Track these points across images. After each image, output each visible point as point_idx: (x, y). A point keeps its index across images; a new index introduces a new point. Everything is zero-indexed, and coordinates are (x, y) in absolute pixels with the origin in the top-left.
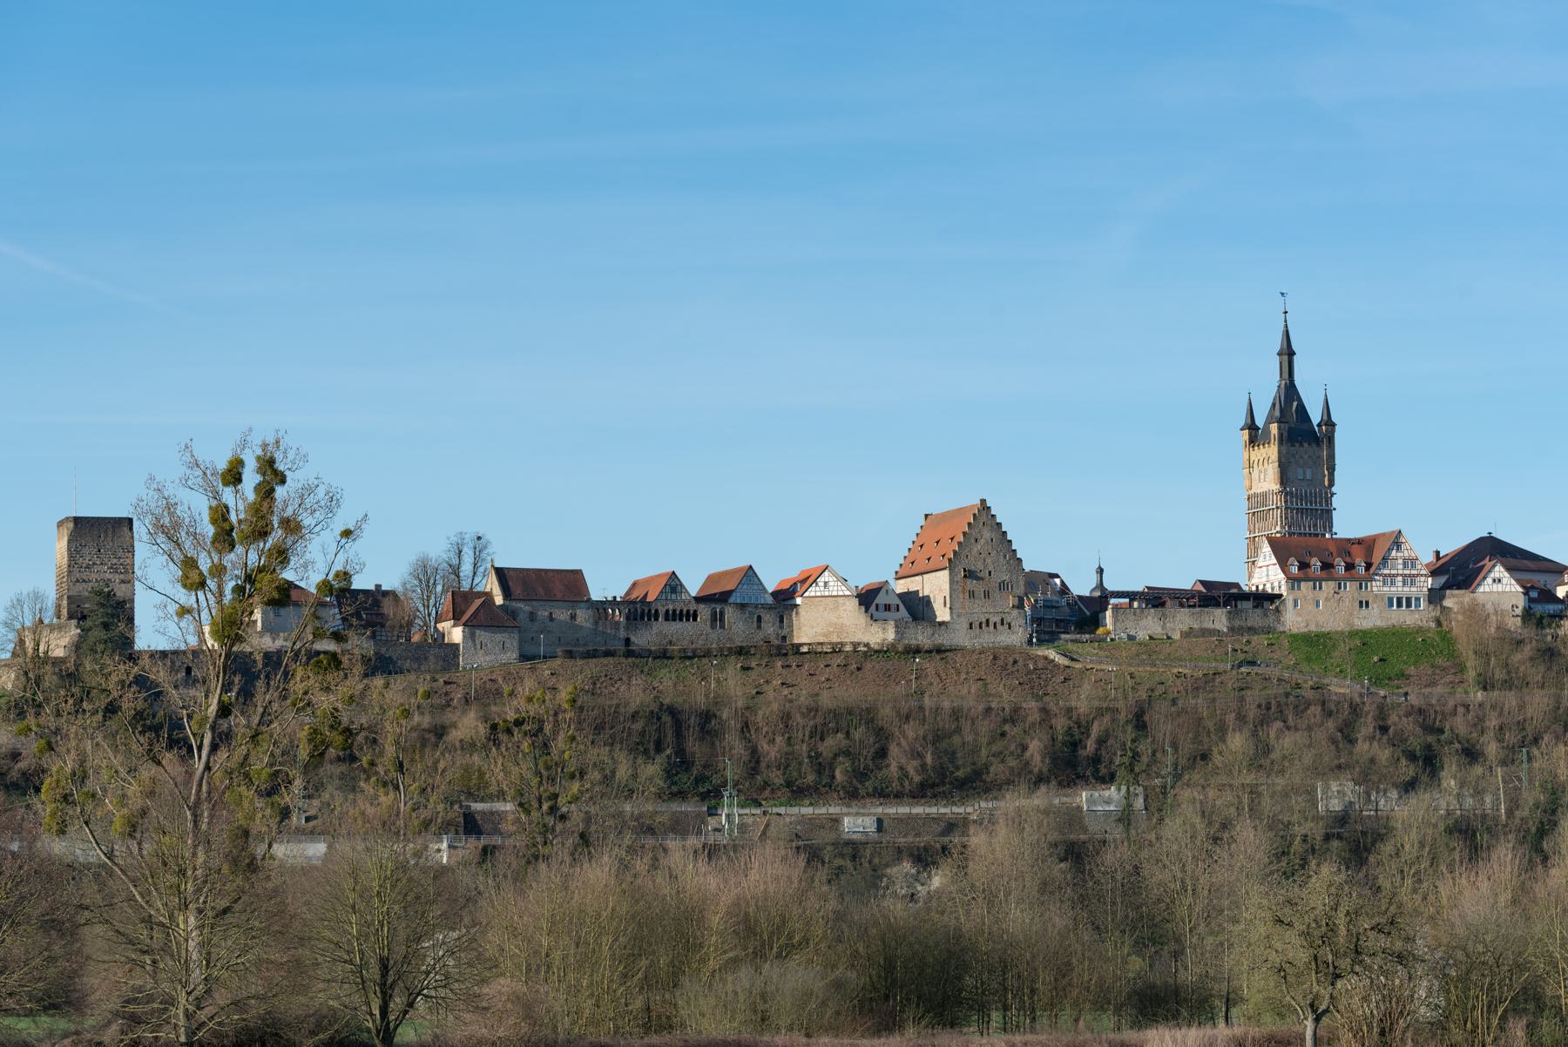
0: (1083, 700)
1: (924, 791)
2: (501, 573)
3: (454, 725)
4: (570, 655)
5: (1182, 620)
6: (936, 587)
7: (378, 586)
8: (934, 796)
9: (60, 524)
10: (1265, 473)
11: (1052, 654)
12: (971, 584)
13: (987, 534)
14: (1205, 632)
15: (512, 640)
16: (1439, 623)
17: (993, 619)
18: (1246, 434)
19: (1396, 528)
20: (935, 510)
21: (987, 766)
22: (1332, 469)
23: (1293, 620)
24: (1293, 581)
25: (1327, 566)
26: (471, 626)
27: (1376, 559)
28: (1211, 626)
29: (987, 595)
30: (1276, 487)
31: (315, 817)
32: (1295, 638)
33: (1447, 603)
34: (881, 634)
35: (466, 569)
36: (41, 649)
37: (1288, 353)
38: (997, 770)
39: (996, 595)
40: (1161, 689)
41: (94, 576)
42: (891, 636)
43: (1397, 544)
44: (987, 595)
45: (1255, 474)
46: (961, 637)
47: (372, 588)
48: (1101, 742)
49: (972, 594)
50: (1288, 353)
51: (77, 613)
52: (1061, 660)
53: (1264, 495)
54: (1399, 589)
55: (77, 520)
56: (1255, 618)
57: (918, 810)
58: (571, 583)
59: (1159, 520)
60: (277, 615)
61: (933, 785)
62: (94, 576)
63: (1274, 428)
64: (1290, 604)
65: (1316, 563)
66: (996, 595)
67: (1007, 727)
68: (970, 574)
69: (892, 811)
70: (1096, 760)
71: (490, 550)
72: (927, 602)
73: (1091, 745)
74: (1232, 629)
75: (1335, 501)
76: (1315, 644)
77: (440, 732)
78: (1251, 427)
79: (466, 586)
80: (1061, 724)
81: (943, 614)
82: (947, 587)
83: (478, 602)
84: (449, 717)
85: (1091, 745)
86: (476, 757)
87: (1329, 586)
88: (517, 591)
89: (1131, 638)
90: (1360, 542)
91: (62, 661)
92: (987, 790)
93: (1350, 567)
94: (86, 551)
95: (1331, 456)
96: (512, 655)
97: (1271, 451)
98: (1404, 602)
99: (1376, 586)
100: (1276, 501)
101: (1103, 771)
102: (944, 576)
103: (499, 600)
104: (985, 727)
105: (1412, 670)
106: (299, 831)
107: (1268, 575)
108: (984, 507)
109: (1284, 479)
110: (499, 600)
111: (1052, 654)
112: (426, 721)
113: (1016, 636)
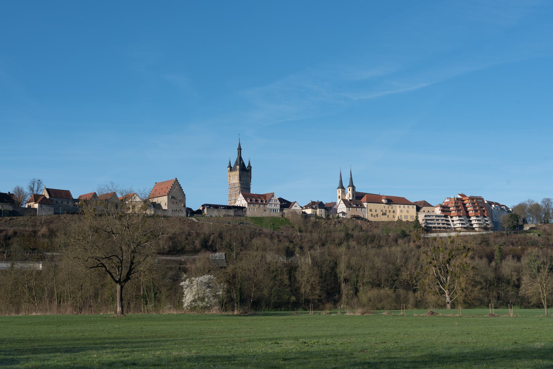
0: (206, 230)
1: (169, 253)
2: (48, 190)
3: (39, 231)
4: (68, 213)
5: (223, 212)
6: (163, 201)
7: (9, 193)
10: (235, 178)
11: (194, 219)
12: (173, 200)
13: (177, 187)
14: (229, 216)
16: (282, 216)
20: (158, 182)
21: (185, 247)
22: (251, 178)
23: (249, 214)
24: (249, 204)
25: (256, 201)
26: (41, 203)
27: (268, 199)
28: (229, 214)
30: (238, 182)
32: (251, 218)
34: (150, 212)
35: (35, 189)
37: (240, 149)
38: (188, 248)
40: (222, 229)
42: (153, 213)
43: (273, 196)
44: (177, 203)
45: (231, 178)
46: (169, 214)
47: (7, 192)
48: (213, 241)
49: (173, 203)
50: (240, 149)
53: (234, 184)
54: (273, 207)
56: (240, 212)
58: (66, 194)
59: (210, 189)
63: (238, 167)
65: (254, 200)
68: (173, 197)
70: (211, 246)
73: (210, 243)
74: (235, 215)
75: (251, 186)
76: (259, 220)
77: (35, 232)
78: (230, 167)
79: (35, 193)
80: (202, 236)
81: (165, 207)
82: (167, 200)
83: (41, 198)
84: (37, 229)
85: (210, 243)
86: (46, 240)
87: (257, 206)
88: (53, 195)
89: (211, 216)
90: (262, 195)
92: (185, 253)
93: (262, 201)
95: (251, 175)
96: (52, 212)
97: (237, 173)
98: (275, 210)
99: (268, 206)
100: (238, 185)
101: (214, 249)
103: (48, 197)
104: (184, 236)
105: (281, 227)
107: (241, 201)
108: (176, 180)
109: (240, 180)
110: (48, 197)
111: (194, 219)
112: (31, 229)
113: (184, 214)
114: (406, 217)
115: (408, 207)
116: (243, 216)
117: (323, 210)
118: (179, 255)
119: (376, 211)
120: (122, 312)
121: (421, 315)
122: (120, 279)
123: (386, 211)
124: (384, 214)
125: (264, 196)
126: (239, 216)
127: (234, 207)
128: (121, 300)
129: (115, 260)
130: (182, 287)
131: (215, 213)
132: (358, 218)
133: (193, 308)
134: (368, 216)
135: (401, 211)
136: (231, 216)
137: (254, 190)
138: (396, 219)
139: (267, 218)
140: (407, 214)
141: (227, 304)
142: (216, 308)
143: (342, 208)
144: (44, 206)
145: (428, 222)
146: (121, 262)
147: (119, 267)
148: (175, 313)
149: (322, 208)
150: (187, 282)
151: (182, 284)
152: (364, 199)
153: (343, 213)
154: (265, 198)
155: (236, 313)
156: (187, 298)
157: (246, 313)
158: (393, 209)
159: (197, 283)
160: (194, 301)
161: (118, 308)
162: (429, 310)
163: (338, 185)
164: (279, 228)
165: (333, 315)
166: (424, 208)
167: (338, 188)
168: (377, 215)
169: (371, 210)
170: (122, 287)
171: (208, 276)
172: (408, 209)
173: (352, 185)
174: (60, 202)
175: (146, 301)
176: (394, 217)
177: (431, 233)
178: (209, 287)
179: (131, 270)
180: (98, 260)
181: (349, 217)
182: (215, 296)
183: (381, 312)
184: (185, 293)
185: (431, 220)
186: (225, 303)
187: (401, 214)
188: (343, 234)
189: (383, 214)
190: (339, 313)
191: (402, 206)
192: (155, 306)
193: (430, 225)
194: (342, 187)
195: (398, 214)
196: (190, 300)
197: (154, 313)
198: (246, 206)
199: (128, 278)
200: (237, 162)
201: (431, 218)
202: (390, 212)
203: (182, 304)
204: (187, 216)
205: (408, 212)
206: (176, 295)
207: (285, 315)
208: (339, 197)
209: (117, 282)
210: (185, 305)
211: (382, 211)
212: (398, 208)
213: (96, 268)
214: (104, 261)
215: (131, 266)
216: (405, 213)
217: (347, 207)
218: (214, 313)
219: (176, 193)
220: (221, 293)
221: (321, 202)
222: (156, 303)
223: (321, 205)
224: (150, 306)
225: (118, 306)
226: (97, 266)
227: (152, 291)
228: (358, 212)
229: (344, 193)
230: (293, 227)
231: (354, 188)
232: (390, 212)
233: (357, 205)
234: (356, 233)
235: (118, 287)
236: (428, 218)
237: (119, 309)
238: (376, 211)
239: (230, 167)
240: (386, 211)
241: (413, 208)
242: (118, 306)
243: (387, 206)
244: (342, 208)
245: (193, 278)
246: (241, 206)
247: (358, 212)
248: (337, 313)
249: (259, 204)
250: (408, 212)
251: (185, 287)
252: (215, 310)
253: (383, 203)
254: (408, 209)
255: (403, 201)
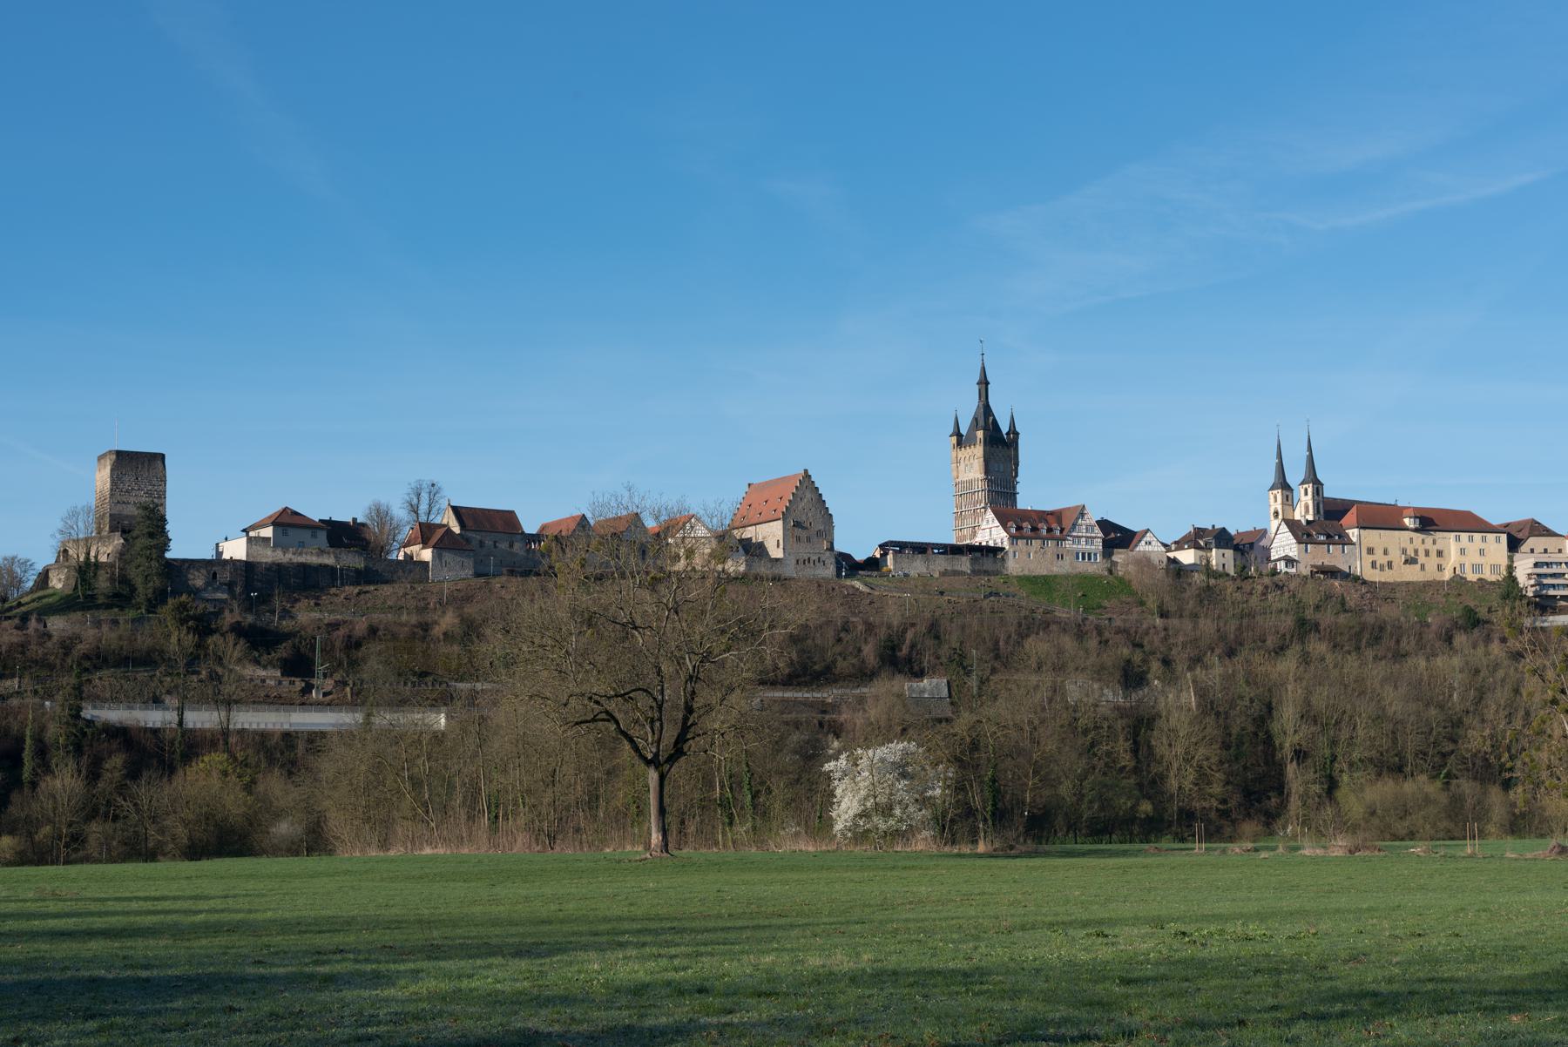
0: (893, 615)
1: (790, 681)
2: (456, 510)
3: (436, 623)
4: (512, 573)
5: (941, 564)
6: (771, 535)
7: (355, 520)
8: (799, 684)
9: (101, 458)
11: (857, 584)
12: (798, 531)
13: (808, 495)
14: (956, 573)
15: (469, 563)
16: (1110, 572)
17: (814, 558)
18: (954, 439)
19: (1079, 503)
20: (757, 480)
21: (834, 662)
22: (1017, 465)
23: (1013, 566)
24: (1013, 538)
25: (1035, 529)
27: (1067, 524)
29: (809, 540)
30: (982, 476)
31: (330, 693)
33: (1115, 558)
34: (736, 565)
35: (423, 507)
36: (92, 554)
37: (984, 383)
38: (842, 666)
39: (815, 539)
41: (132, 500)
42: (742, 568)
43: (1082, 515)
46: (789, 571)
48: (913, 646)
49: (798, 539)
50: (984, 383)
51: (119, 525)
52: (862, 587)
53: (971, 482)
54: (1083, 546)
55: (119, 453)
56: (988, 564)
57: (788, 695)
58: (508, 520)
59: (902, 497)
60: (285, 534)
61: (798, 676)
62: (132, 500)
63: (980, 434)
64: (1011, 555)
65: (1027, 526)
66: (815, 539)
67: (843, 635)
69: (770, 694)
70: (909, 660)
71: (443, 493)
72: (761, 546)
73: (905, 650)
75: (1019, 488)
77: (425, 627)
78: (958, 434)
79: (423, 519)
80: (882, 633)
81: (776, 552)
83: (441, 532)
84: (429, 617)
85: (905, 650)
87: (1036, 543)
88: (469, 523)
89: (906, 575)
90: (1052, 513)
91: (112, 565)
92: (835, 681)
93: (1050, 530)
94: (126, 478)
97: (979, 450)
98: (1086, 556)
99: (1068, 544)
101: (916, 668)
102: (779, 525)
103: (457, 529)
104: (830, 633)
105: (1106, 603)
106: (319, 704)
107: (991, 532)
108: (807, 475)
109: (987, 472)
110: (457, 529)
111: (857, 584)
112: (414, 619)
113: (829, 571)
114: (1477, 568)
115: (1484, 540)
116: (997, 573)
117: (1229, 553)
118: (819, 687)
119: (1386, 552)
120: (665, 846)
121: (1529, 856)
122: (656, 755)
123: (1416, 552)
124: (1411, 561)
125: (1057, 515)
126: (986, 573)
127: (972, 549)
128: (662, 811)
129: (643, 701)
130: (828, 777)
131: (917, 567)
132: (1332, 573)
133: (860, 836)
134: (1360, 566)
135: (1463, 552)
136: (962, 573)
137: (1029, 497)
138: (1447, 575)
139: (1067, 577)
140: (1478, 560)
141: (955, 824)
142: (925, 834)
143: (1283, 545)
144: (448, 556)
145: (1545, 581)
146: (660, 707)
147: (652, 721)
148: (811, 849)
149: (1227, 547)
150: (843, 761)
151: (828, 767)
152: (1350, 517)
153: (1289, 561)
154: (1060, 522)
155: (981, 848)
156: (843, 806)
157: (1012, 847)
158: (1438, 546)
159: (872, 765)
160: (864, 814)
161: (654, 836)
162: (1553, 842)
163: (1271, 478)
164: (1100, 607)
165: (1264, 855)
166: (1532, 542)
167: (1272, 488)
168: (1390, 565)
169: (1370, 551)
170: (662, 778)
171: (901, 746)
172: (1483, 546)
173: (1312, 478)
174: (489, 543)
175: (731, 817)
176: (1440, 568)
177: (1554, 613)
178: (904, 775)
179: (685, 728)
180: (597, 702)
181: (1306, 571)
182: (923, 802)
183: (1407, 848)
184: (838, 792)
185: (1554, 575)
186: (952, 821)
187: (1463, 559)
188: (1288, 622)
189: (1406, 562)
190: (1281, 850)
191: (1464, 536)
192: (754, 828)
193: (1551, 592)
194: (1283, 484)
195: (1453, 559)
196: (851, 813)
197: (754, 850)
198: (1006, 545)
199: (678, 752)
200: (976, 419)
201: (1555, 570)
202: (1427, 553)
203: (830, 823)
204: (839, 575)
205: (1482, 552)
206: (813, 798)
207: (1125, 853)
208: (1276, 514)
209: (648, 762)
210: (839, 826)
211: (1404, 551)
212: (1452, 540)
213: (592, 726)
214: (612, 706)
215: (686, 719)
216: (1473, 558)
217: (1299, 542)
218: (920, 847)
219: (807, 510)
220: (938, 791)
221: (1224, 530)
222: (759, 822)
223: (1222, 538)
224: (742, 829)
225: (654, 829)
226: (594, 720)
227: (746, 787)
228: (1333, 556)
229: (1289, 500)
230: (1142, 603)
231: (1318, 486)
232: (1427, 553)
233: (1329, 536)
234: (1327, 618)
235: (653, 776)
236: (1545, 570)
237: (656, 838)
238: (1386, 552)
239: (958, 434)
240: (1416, 552)
241: (1498, 540)
242: (654, 829)
243: (1418, 537)
244: (1283, 545)
245: (860, 751)
246: (991, 544)
247: (1333, 556)
248: (1274, 849)
249: (1044, 539)
250: (1482, 552)
251: (837, 775)
252: (923, 842)
253: (1407, 529)
254: (1483, 546)
255: (1467, 523)
